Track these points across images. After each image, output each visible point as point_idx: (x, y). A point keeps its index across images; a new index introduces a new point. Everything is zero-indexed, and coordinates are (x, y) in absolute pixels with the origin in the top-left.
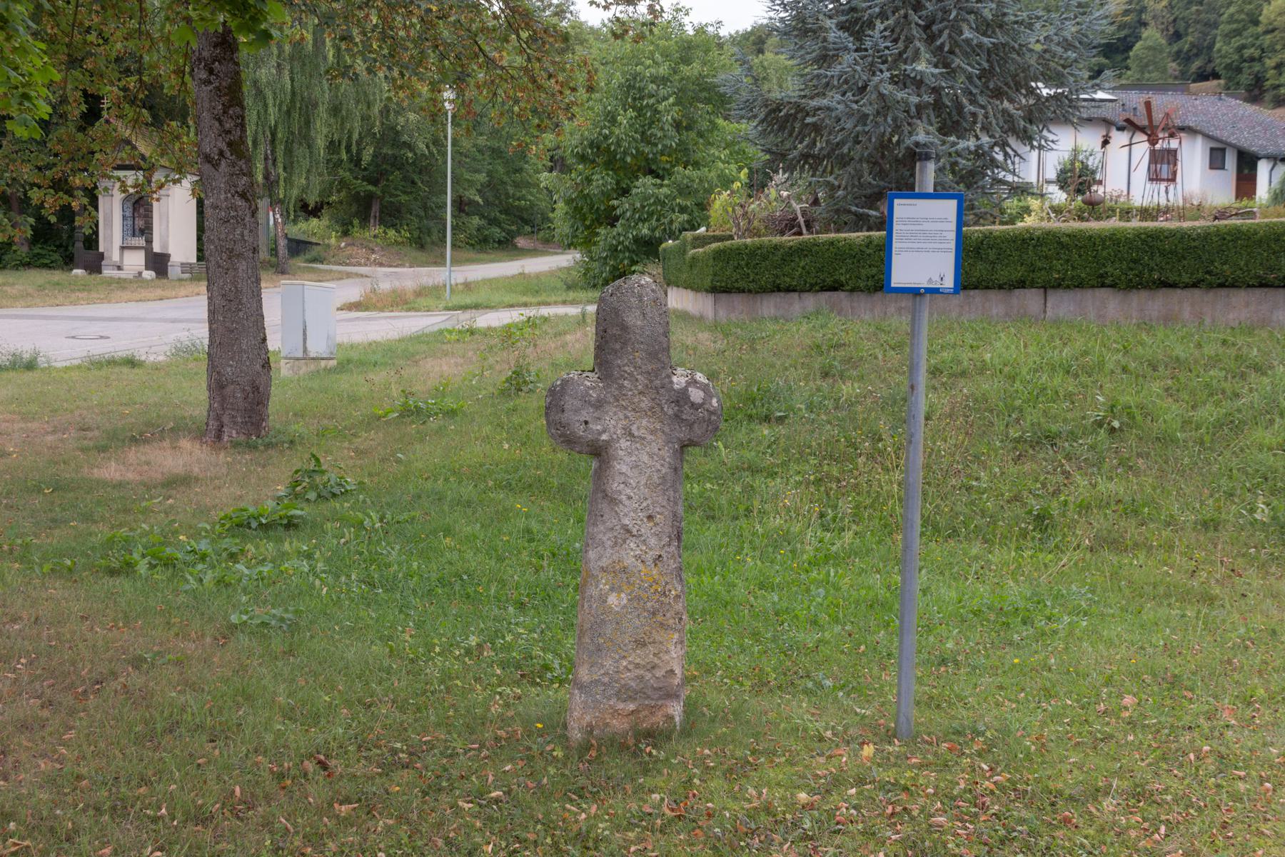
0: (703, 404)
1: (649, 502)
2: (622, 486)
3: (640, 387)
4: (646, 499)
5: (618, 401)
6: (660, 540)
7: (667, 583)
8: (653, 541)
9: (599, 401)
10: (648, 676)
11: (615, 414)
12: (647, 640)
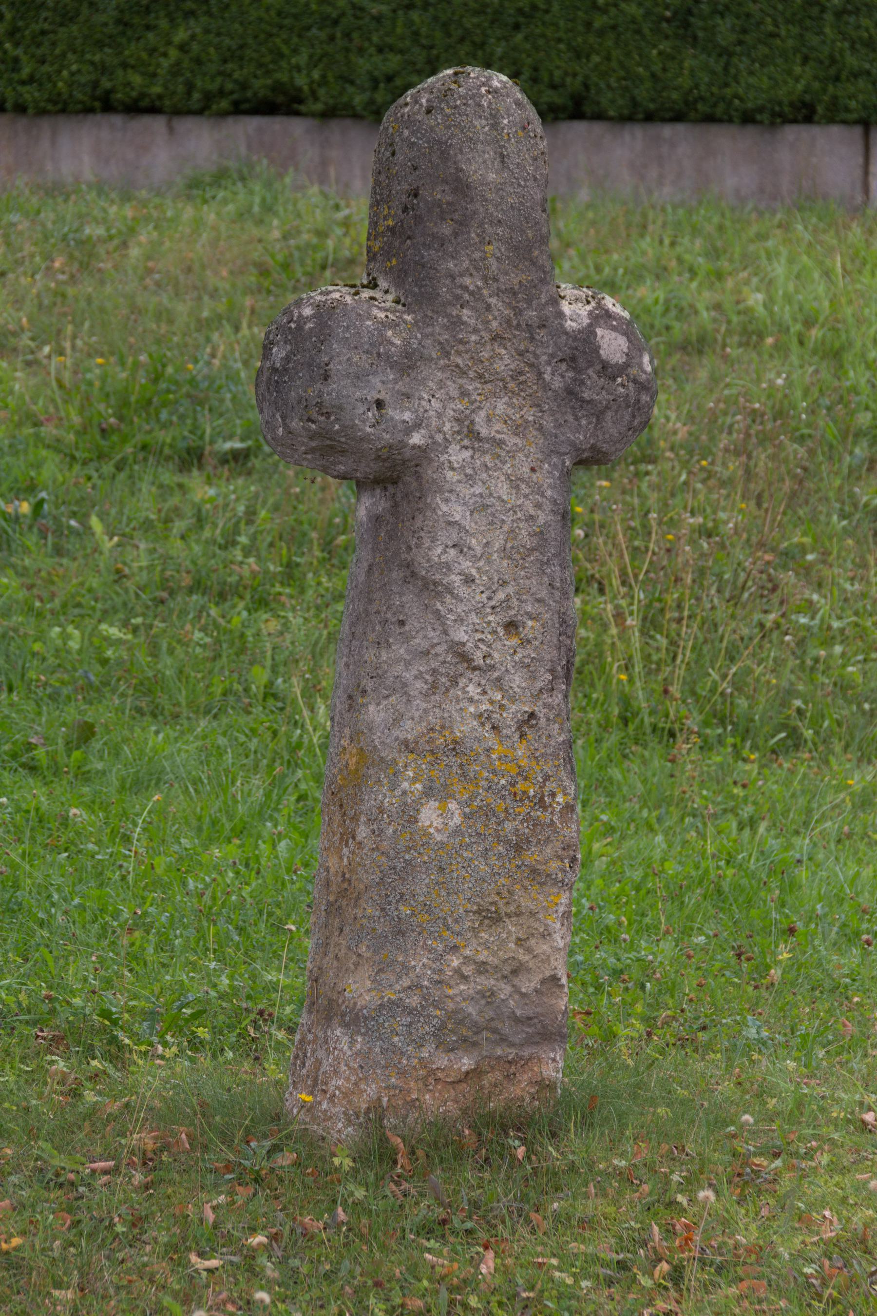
0: (627, 365)
1: (510, 589)
2: (452, 552)
3: (495, 324)
4: (504, 583)
5: (447, 355)
6: (533, 678)
7: (547, 778)
8: (517, 681)
9: (408, 355)
10: (505, 990)
12: (503, 909)
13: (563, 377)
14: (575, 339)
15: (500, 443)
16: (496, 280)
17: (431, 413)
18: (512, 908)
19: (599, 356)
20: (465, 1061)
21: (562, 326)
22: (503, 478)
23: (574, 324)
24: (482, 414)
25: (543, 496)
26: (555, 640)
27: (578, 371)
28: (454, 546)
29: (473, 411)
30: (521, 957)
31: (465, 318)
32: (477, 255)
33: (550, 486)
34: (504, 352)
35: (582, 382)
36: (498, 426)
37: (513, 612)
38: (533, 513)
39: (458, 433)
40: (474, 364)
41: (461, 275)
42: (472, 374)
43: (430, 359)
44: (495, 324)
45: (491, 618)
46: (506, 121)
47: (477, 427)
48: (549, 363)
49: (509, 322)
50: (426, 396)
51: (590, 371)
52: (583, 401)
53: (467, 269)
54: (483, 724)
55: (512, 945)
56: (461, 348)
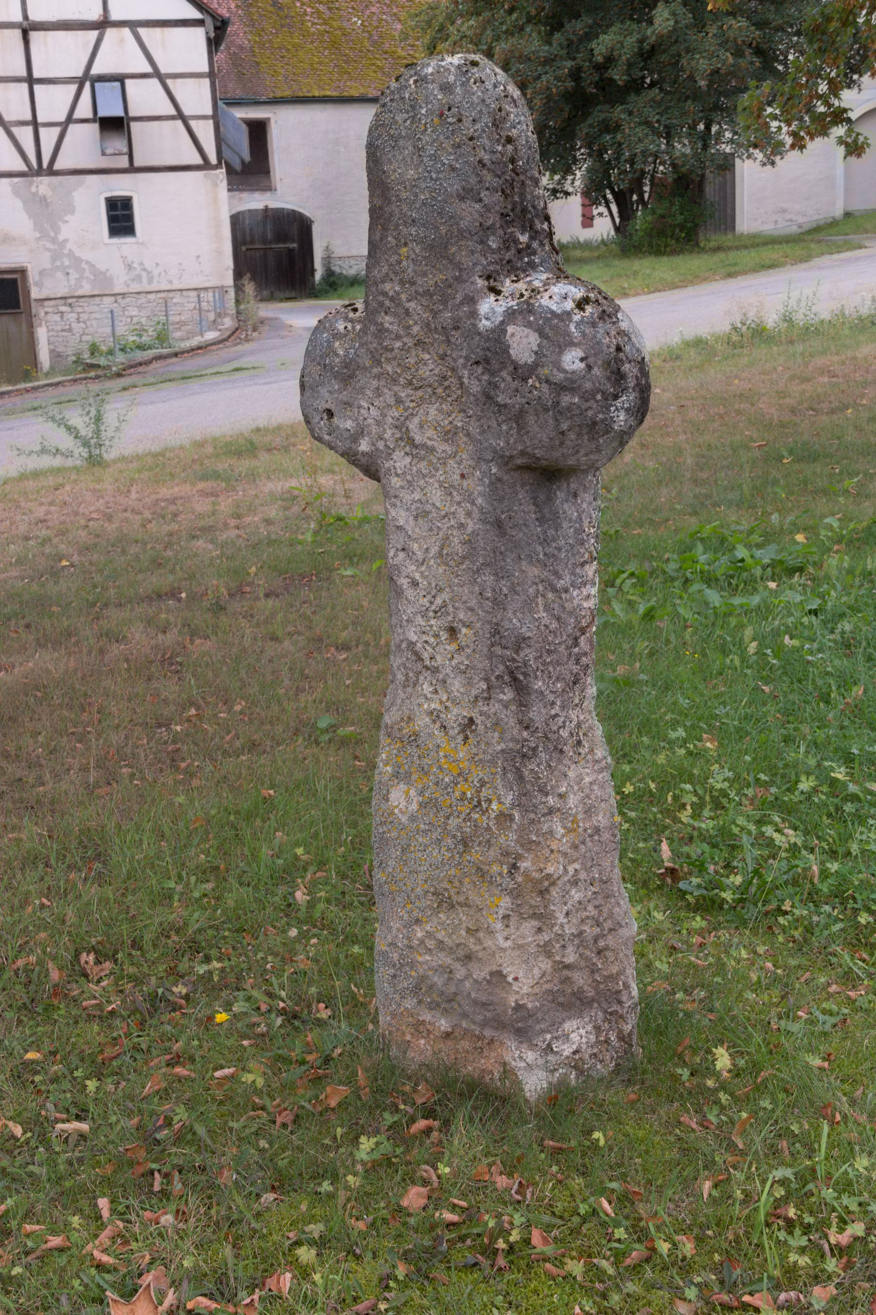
0: (536, 365)
1: (445, 596)
2: (402, 555)
3: (416, 329)
4: (441, 590)
5: (379, 363)
6: (469, 683)
7: (483, 783)
8: (457, 685)
9: (346, 366)
10: (460, 972)
11: (378, 392)
12: (455, 898)
13: (480, 380)
14: (488, 339)
15: (433, 450)
16: (413, 283)
17: (370, 421)
18: (461, 899)
19: (509, 356)
20: (443, 1022)
21: (474, 326)
22: (436, 485)
23: (487, 323)
24: (416, 420)
25: (473, 503)
26: (485, 650)
27: (493, 374)
28: (403, 549)
29: (407, 418)
30: (472, 946)
31: (387, 325)
32: (394, 259)
33: (479, 493)
34: (427, 356)
35: (496, 386)
36: (430, 433)
37: (450, 618)
38: (463, 521)
39: (401, 439)
40: (404, 371)
41: (383, 282)
42: (402, 381)
43: (365, 369)
44: (416, 329)
45: (433, 622)
46: (423, 111)
47: (412, 434)
48: (464, 366)
49: (428, 325)
50: (366, 405)
51: (504, 374)
52: (500, 406)
53: (387, 274)
54: (434, 722)
55: (463, 933)
56: (389, 355)
